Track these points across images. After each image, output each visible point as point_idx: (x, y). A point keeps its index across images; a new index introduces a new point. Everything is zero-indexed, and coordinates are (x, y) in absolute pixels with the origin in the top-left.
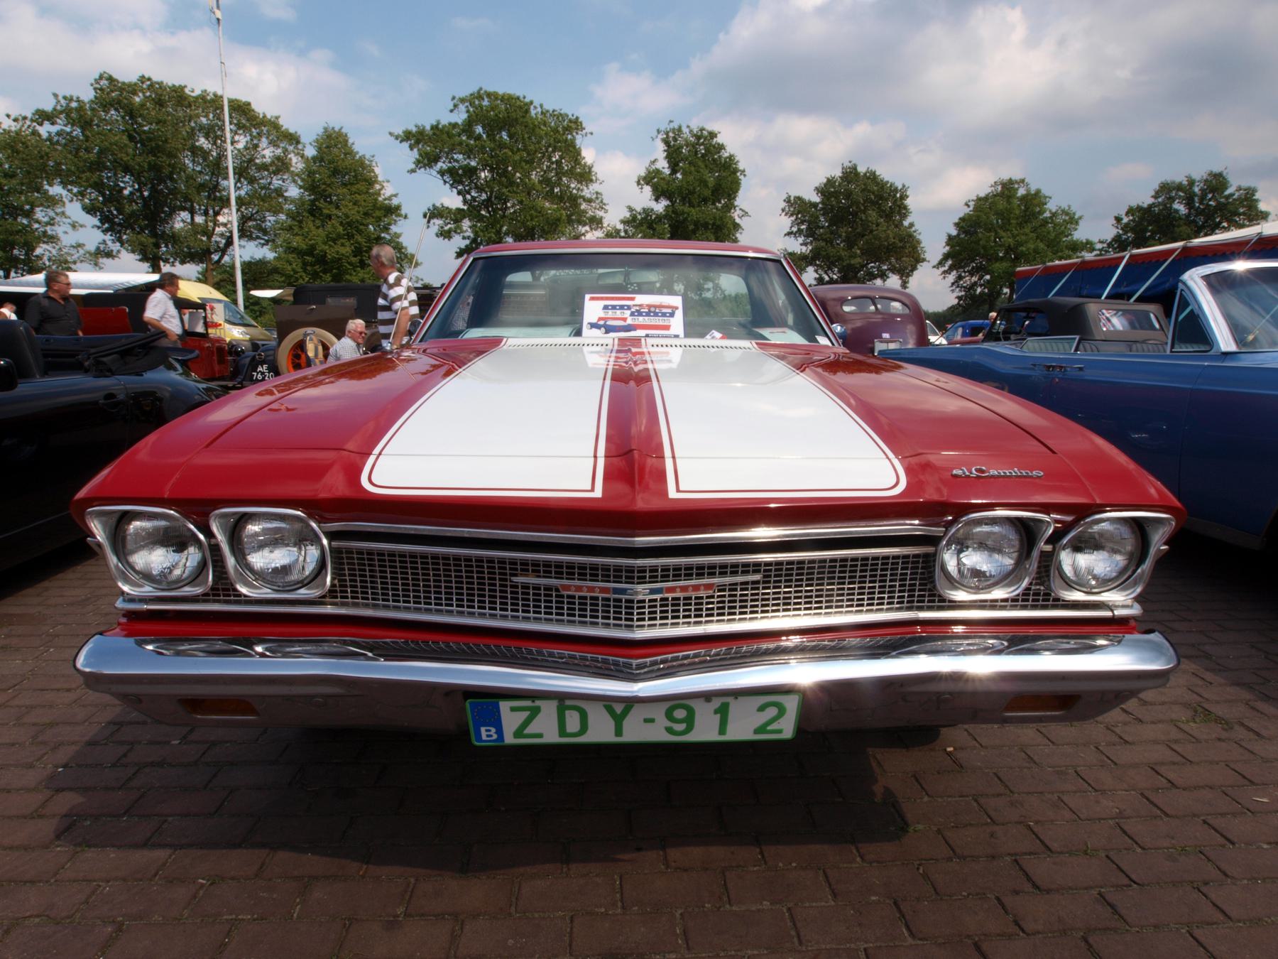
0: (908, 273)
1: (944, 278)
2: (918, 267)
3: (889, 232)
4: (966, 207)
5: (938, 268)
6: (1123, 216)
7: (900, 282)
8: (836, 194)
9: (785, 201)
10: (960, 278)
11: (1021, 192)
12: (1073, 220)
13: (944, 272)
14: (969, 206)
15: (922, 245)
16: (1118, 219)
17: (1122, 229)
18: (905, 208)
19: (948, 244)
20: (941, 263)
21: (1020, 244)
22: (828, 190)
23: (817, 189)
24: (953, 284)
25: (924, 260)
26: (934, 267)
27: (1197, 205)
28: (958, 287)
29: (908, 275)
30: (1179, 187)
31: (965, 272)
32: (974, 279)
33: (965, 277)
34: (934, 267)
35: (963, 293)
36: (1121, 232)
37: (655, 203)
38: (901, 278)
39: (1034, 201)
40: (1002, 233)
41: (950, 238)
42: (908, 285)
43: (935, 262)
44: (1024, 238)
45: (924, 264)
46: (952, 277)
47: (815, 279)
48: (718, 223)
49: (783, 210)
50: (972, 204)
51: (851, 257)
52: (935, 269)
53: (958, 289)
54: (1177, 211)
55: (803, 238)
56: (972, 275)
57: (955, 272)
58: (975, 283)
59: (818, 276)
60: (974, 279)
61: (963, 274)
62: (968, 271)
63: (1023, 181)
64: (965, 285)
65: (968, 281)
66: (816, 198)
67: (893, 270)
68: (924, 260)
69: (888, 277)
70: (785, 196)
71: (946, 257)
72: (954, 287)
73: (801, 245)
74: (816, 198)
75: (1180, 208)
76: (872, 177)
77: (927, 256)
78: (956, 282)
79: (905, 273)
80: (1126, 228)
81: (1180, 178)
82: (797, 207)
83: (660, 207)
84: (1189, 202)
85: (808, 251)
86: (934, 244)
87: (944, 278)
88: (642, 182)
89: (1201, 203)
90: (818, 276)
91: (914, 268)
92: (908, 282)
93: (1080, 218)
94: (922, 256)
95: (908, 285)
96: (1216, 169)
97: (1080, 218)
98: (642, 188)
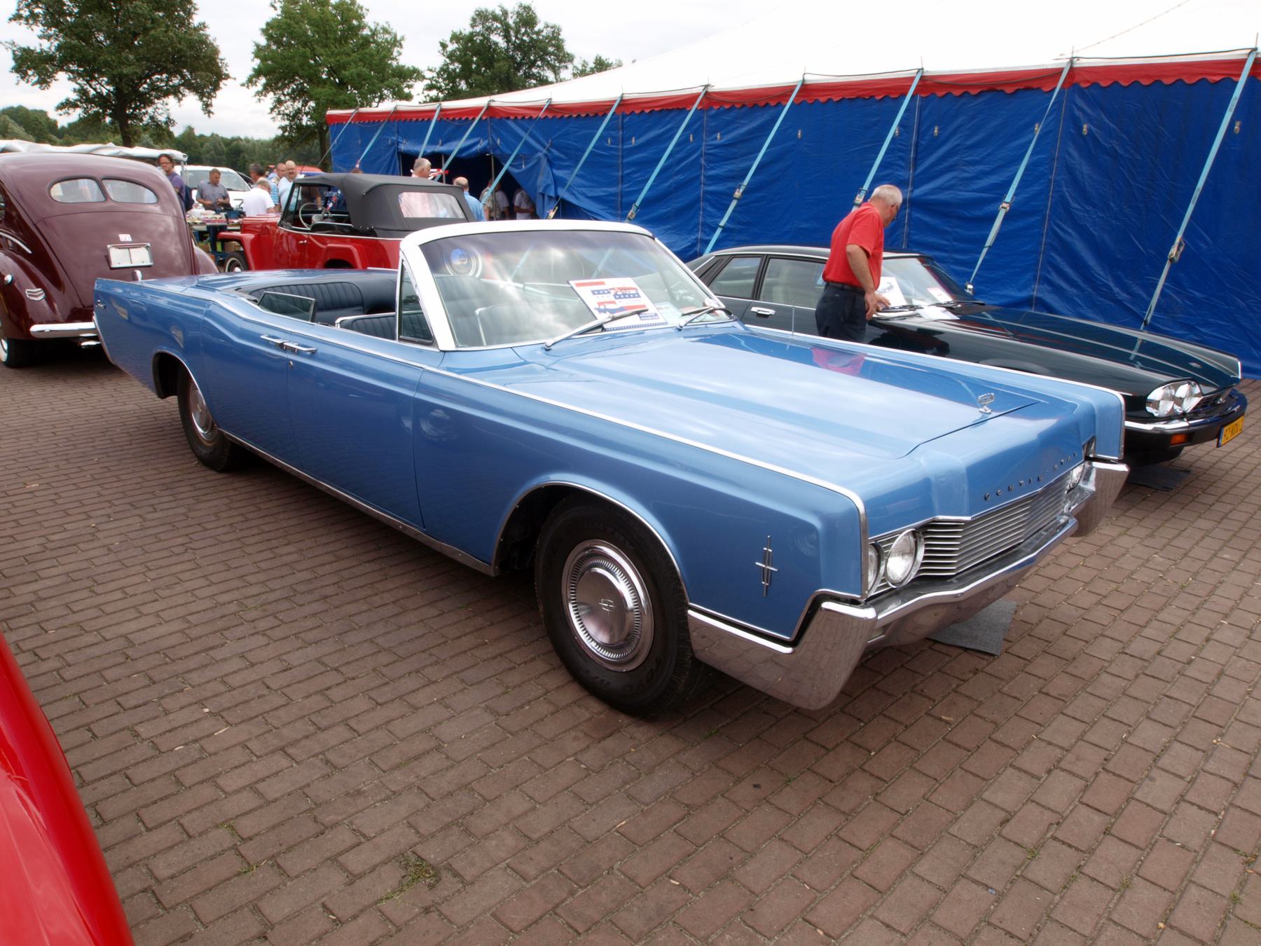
0: (209, 93)
1: (259, 100)
2: (221, 84)
4: (273, 9)
5: (248, 87)
6: (448, 43)
7: (200, 104)
10: (280, 102)
13: (258, 93)
14: (275, 8)
16: (444, 46)
17: (448, 57)
20: (251, 81)
21: (344, 66)
24: (272, 110)
25: (227, 77)
26: (243, 85)
27: (514, 39)
28: (279, 114)
29: (210, 97)
30: (495, 18)
31: (285, 95)
32: (298, 105)
33: (286, 102)
34: (243, 85)
35: (287, 123)
36: (448, 61)
38: (201, 99)
40: (319, 50)
42: (211, 109)
43: (244, 80)
47: (75, 91)
53: (280, 117)
54: (496, 44)
55: (41, 27)
56: (294, 99)
57: (271, 95)
58: (299, 111)
59: (77, 87)
60: (298, 105)
61: (283, 98)
62: (288, 94)
64: (287, 112)
65: (291, 106)
68: (227, 77)
69: (184, 95)
71: (258, 73)
72: (274, 114)
73: (40, 37)
75: (498, 39)
77: (230, 70)
78: (275, 107)
80: (451, 56)
85: (53, 49)
87: (259, 100)
89: (516, 37)
91: (216, 87)
92: (211, 105)
93: (403, 39)
95: (211, 109)
97: (403, 39)
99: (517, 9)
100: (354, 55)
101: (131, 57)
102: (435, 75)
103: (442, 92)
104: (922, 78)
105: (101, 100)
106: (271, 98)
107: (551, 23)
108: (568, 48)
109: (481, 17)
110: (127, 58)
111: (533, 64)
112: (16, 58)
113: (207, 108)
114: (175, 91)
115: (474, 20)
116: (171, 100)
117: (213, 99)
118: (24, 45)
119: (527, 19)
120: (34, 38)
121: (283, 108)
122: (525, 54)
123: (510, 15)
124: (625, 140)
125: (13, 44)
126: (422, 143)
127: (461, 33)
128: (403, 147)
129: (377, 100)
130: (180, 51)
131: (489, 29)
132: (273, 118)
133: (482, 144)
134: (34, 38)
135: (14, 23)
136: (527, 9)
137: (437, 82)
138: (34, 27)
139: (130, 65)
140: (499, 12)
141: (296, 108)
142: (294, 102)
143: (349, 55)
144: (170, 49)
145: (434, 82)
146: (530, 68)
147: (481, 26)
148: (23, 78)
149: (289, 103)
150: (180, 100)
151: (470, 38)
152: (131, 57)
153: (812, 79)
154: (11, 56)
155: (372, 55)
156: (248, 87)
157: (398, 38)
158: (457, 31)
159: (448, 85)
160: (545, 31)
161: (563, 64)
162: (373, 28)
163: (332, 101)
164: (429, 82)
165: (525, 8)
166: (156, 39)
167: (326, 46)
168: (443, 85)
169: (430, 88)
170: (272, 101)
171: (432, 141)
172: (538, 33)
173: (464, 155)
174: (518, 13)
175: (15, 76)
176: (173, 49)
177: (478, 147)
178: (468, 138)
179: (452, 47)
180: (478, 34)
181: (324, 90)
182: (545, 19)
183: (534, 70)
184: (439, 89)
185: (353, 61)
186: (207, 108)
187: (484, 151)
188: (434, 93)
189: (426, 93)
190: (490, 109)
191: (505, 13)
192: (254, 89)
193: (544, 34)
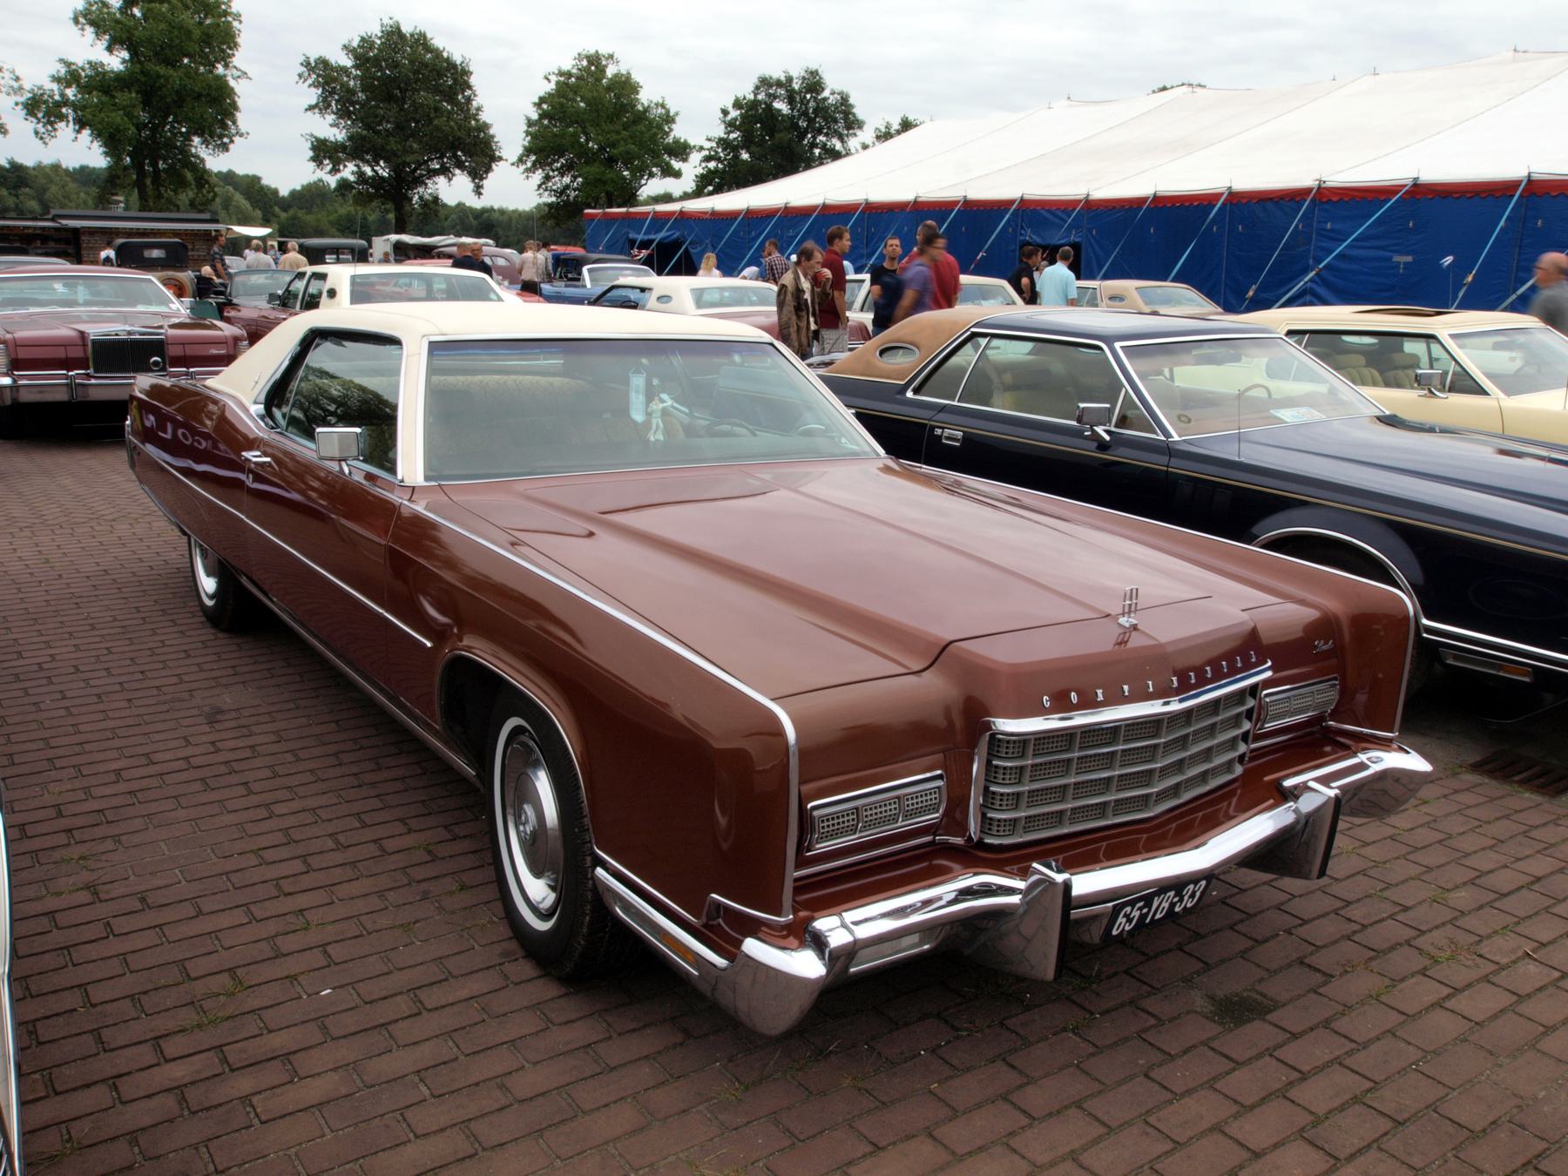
1: (528, 177)
2: (494, 166)
3: (452, 123)
4: (546, 81)
5: (518, 166)
6: (730, 109)
7: (472, 185)
8: (376, 61)
9: (302, 64)
10: (547, 178)
11: (610, 71)
12: (669, 119)
13: (527, 170)
15: (495, 140)
16: (725, 112)
18: (470, 87)
19: (528, 133)
20: (521, 160)
22: (363, 54)
23: (345, 47)
24: (540, 186)
25: (500, 159)
26: (513, 164)
28: (546, 190)
29: (482, 179)
30: (779, 84)
31: (553, 171)
32: (567, 180)
34: (513, 164)
37: (106, 53)
38: (473, 181)
39: (625, 86)
40: (590, 129)
41: (530, 123)
43: (515, 159)
44: (615, 137)
45: (501, 163)
46: (538, 176)
47: (353, 173)
48: (214, 93)
49: (300, 76)
50: (554, 79)
51: (405, 151)
52: (514, 167)
53: (546, 193)
58: (567, 187)
61: (551, 174)
62: (557, 169)
63: (611, 57)
64: (554, 187)
66: (347, 61)
67: (460, 166)
68: (500, 159)
69: (454, 175)
70: (302, 59)
71: (528, 151)
72: (541, 191)
73: (331, 125)
74: (347, 61)
75: (781, 106)
76: (421, 41)
77: (504, 154)
78: (544, 183)
79: (478, 173)
80: (731, 125)
81: (777, 74)
82: (322, 73)
83: (115, 62)
84: (791, 98)
86: (510, 136)
87: (528, 177)
88: (82, 20)
90: (355, 169)
91: (488, 169)
92: (482, 187)
93: (677, 114)
94: (497, 153)
95: (482, 191)
96: (813, 67)
97: (677, 114)
98: (83, 29)
99: (803, 74)
100: (625, 132)
101: (415, 146)
102: (714, 145)
103: (722, 162)
104: (867, 203)
105: (377, 181)
106: (538, 176)
107: (838, 88)
108: (859, 112)
109: (765, 82)
110: (411, 147)
111: (820, 132)
112: (314, 148)
113: (478, 190)
114: (444, 171)
115: (757, 88)
116: (441, 180)
117: (485, 181)
118: (322, 137)
119: (814, 83)
120: (330, 129)
121: (550, 184)
122: (811, 121)
123: (795, 81)
124: (750, 233)
125: (312, 135)
126: (639, 233)
127: (745, 98)
128: (631, 236)
129: (646, 177)
130: (459, 138)
131: (774, 97)
132: (540, 194)
133: (677, 234)
134: (330, 129)
135: (309, 113)
136: (814, 73)
137: (716, 152)
138: (326, 116)
139: (413, 153)
140: (783, 79)
141: (564, 184)
142: (563, 177)
143: (618, 133)
144: (450, 138)
145: (712, 153)
146: (814, 137)
147: (763, 94)
148: (318, 166)
149: (557, 179)
150: (450, 180)
151: (754, 104)
152: (415, 146)
153: (828, 202)
154: (309, 145)
155: (642, 133)
156: (518, 166)
157: (671, 114)
158: (740, 95)
159: (729, 154)
160: (831, 97)
161: (851, 132)
162: (646, 105)
163: (600, 180)
164: (707, 153)
165: (812, 73)
166: (438, 129)
167: (598, 125)
168: (722, 155)
169: (708, 159)
170: (540, 177)
171: (645, 233)
172: (825, 99)
173: (666, 241)
174: (804, 78)
175: (313, 164)
176: (454, 137)
177: (675, 236)
178: (667, 231)
179: (734, 113)
180: (760, 102)
181: (593, 169)
182: (833, 84)
183: (822, 138)
184: (719, 160)
185: (622, 139)
186: (478, 190)
187: (678, 239)
188: (712, 165)
189: (704, 165)
190: (682, 213)
191: (790, 79)
192: (522, 168)
193: (830, 101)
